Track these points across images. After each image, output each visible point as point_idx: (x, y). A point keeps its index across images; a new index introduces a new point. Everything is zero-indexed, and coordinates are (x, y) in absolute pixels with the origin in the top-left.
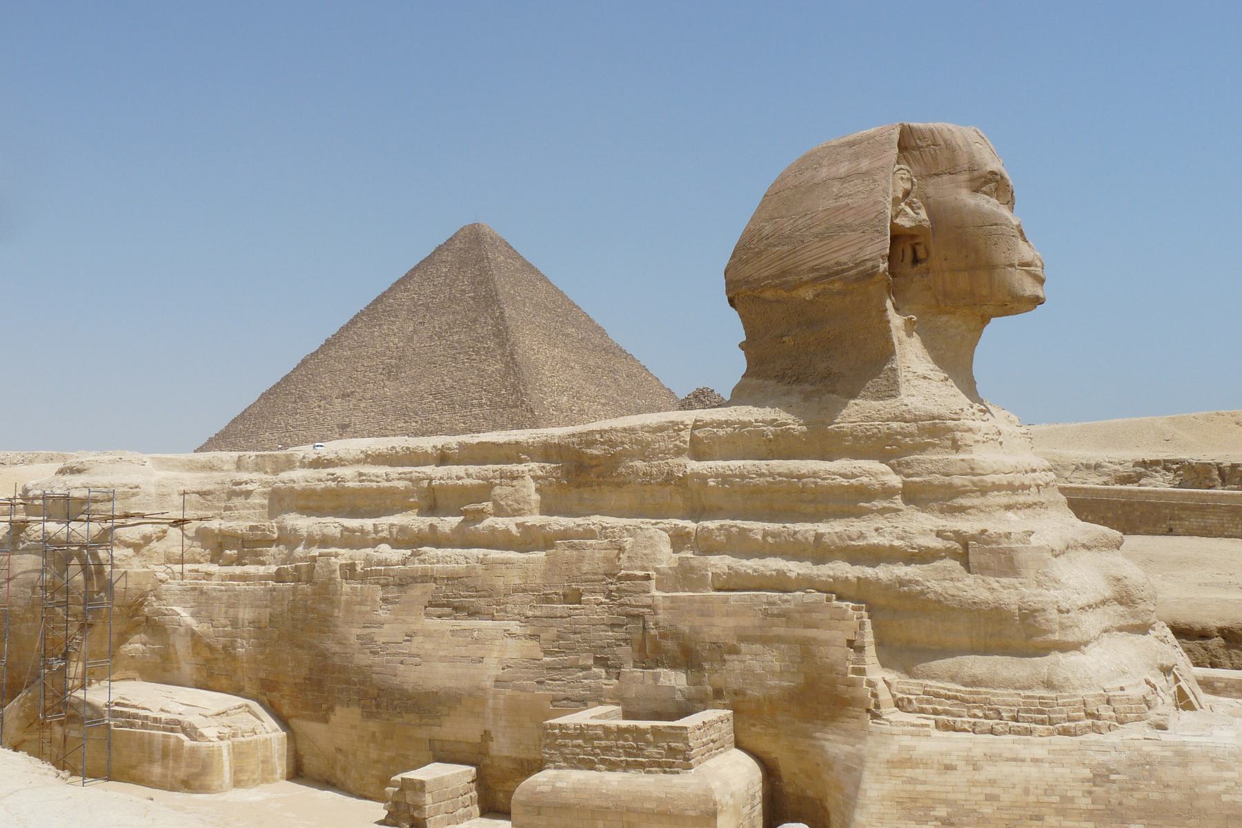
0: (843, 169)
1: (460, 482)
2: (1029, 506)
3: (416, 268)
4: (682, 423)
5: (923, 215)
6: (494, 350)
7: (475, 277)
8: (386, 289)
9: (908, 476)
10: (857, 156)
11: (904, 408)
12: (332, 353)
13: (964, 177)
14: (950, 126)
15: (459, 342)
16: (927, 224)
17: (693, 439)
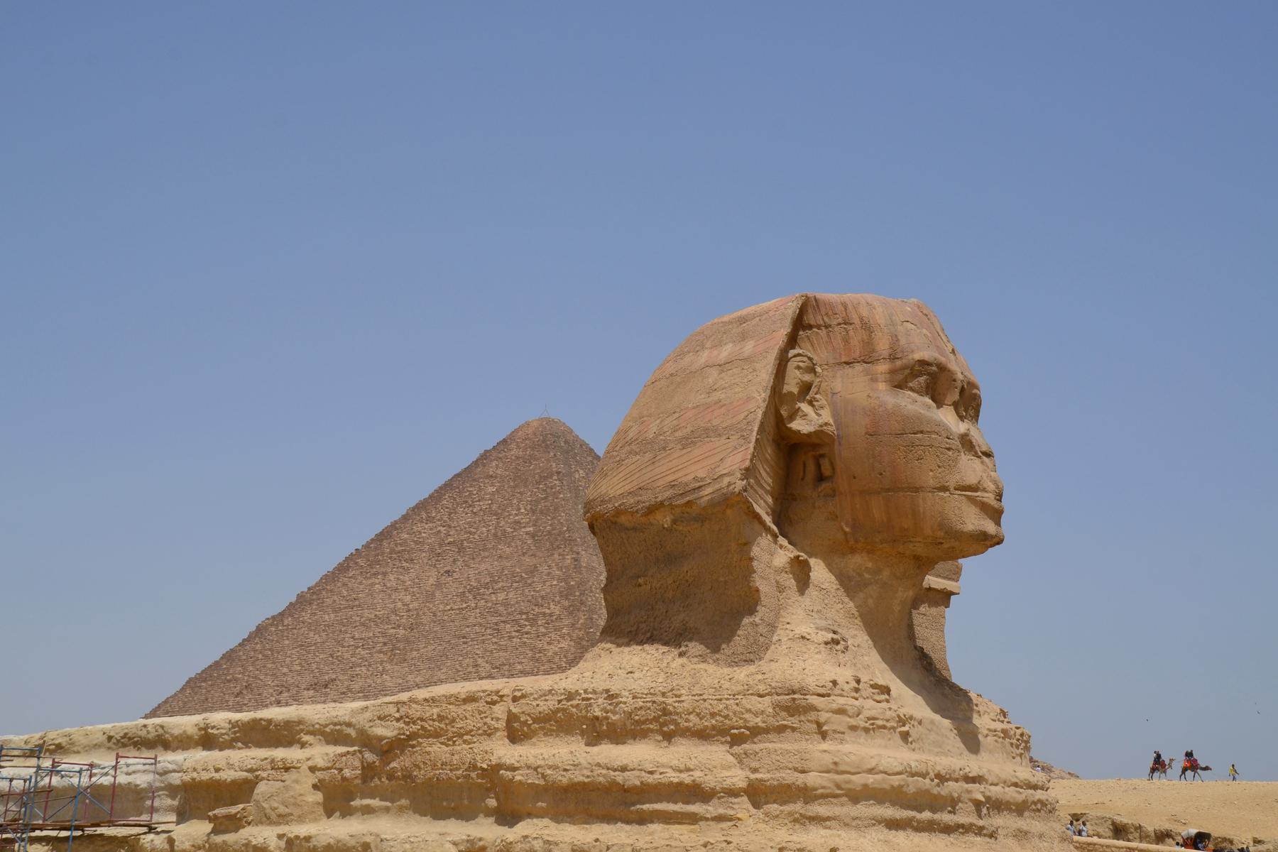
0: (726, 352)
1: (217, 776)
2: (948, 829)
3: (448, 486)
4: (497, 692)
5: (826, 416)
6: (559, 618)
7: (538, 502)
8: (397, 517)
9: (755, 770)
10: (743, 337)
11: (760, 677)
12: (306, 616)
13: (882, 367)
14: (870, 297)
15: (506, 604)
16: (831, 429)
17: (512, 718)
